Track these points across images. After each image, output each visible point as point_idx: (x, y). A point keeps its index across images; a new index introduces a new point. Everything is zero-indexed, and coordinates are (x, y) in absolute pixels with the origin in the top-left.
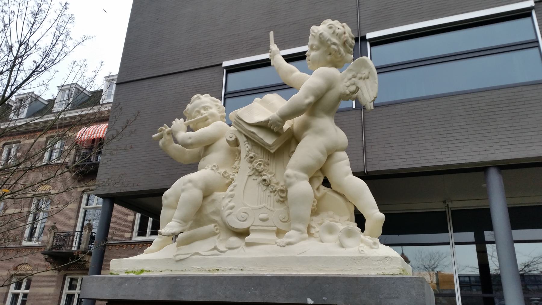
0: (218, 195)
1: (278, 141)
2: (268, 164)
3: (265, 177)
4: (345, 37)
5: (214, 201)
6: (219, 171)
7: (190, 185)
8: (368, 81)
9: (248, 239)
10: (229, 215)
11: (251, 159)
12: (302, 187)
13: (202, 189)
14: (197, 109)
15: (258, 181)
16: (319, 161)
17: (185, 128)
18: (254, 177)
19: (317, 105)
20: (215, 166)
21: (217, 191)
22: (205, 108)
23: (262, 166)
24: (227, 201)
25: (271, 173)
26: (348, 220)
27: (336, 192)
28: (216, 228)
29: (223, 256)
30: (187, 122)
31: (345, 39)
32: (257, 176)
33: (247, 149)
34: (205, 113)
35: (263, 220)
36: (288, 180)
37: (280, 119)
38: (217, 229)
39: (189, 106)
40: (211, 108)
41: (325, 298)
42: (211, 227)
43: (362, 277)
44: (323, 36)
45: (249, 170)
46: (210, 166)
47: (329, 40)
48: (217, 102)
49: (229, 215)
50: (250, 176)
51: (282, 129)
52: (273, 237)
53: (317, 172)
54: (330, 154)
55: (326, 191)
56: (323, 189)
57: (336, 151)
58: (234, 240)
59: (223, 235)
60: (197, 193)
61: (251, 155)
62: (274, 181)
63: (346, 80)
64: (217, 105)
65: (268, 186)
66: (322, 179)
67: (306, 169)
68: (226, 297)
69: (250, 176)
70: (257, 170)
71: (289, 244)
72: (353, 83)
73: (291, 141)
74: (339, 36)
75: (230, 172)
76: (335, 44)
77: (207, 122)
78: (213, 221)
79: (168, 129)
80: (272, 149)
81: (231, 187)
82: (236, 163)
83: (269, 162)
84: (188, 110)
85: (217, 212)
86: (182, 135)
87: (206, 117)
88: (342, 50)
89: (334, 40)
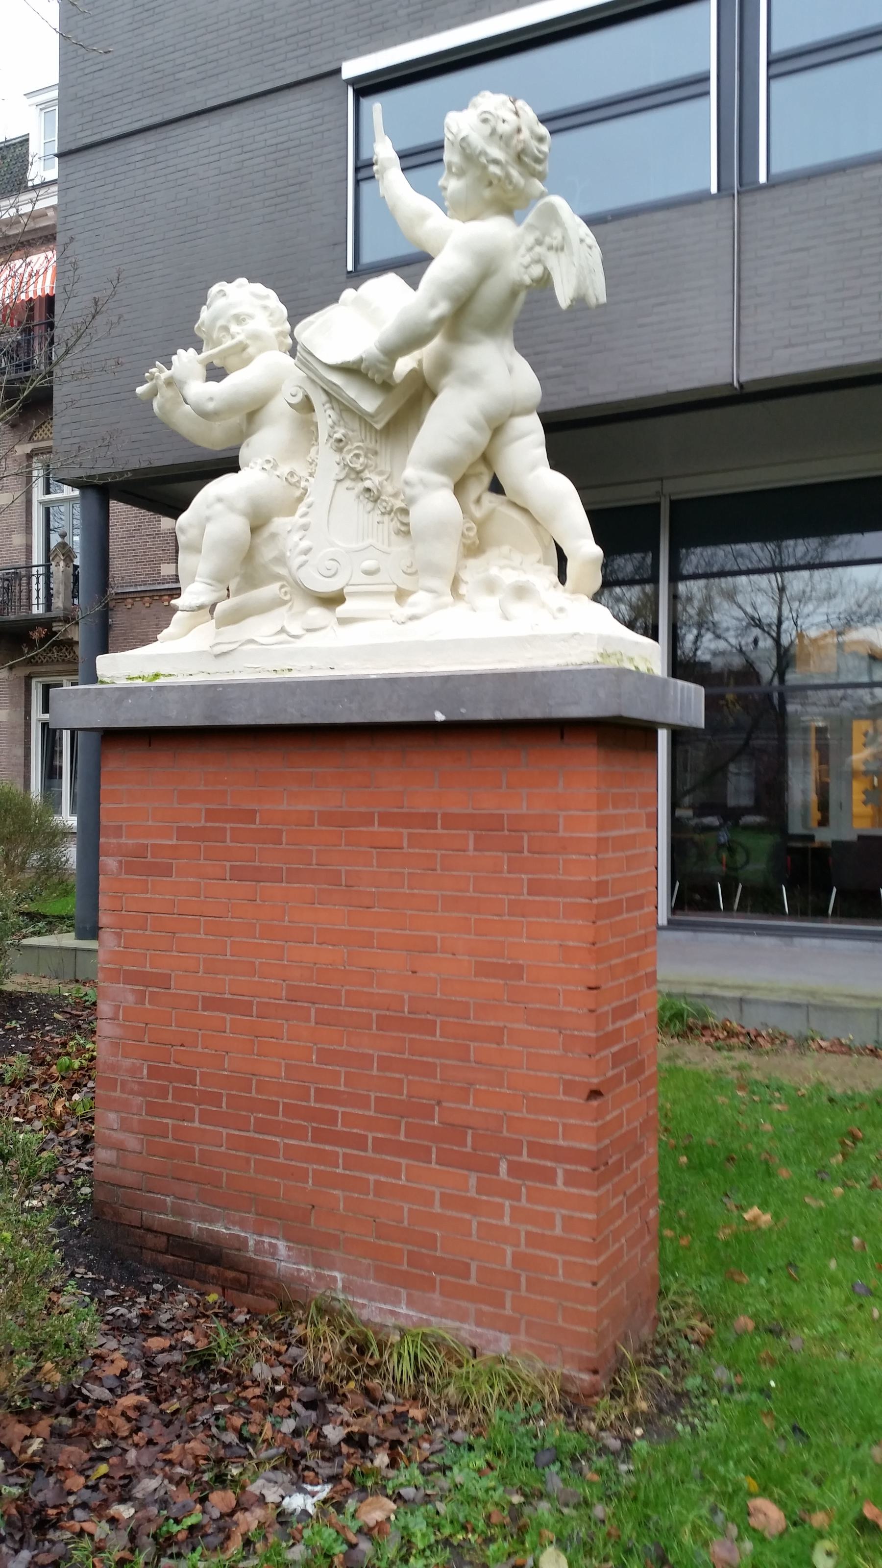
0: (279, 523)
1: (391, 400)
2: (376, 453)
3: (368, 484)
4: (519, 141)
5: (274, 536)
6: (278, 473)
7: (219, 507)
8: (562, 255)
9: (342, 610)
10: (301, 566)
11: (340, 445)
12: (438, 502)
13: (245, 514)
14: (221, 322)
15: (356, 491)
16: (470, 445)
17: (201, 371)
18: (348, 483)
19: (463, 317)
20: (268, 461)
21: (279, 514)
22: (239, 319)
23: (362, 459)
24: (295, 537)
25: (381, 473)
26: (539, 562)
27: (515, 505)
28: (283, 590)
29: (298, 644)
30: (204, 354)
31: (520, 147)
32: (353, 480)
33: (330, 421)
34: (240, 333)
35: (368, 573)
36: (409, 491)
37: (382, 357)
38: (286, 593)
39: (205, 314)
40: (251, 317)
41: (463, 711)
42: (271, 590)
43: (524, 673)
44: (469, 145)
45: (337, 469)
46: (260, 461)
47: (483, 153)
48: (267, 297)
49: (301, 566)
50: (339, 481)
51: (391, 376)
52: (390, 604)
53: (472, 465)
54: (497, 427)
55: (493, 505)
56: (491, 500)
57: (513, 415)
58: (317, 614)
59: (298, 604)
60: (238, 525)
61: (338, 436)
62: (389, 489)
63: (523, 250)
64: (265, 308)
65: (375, 501)
66: (486, 480)
67: (443, 466)
68: (303, 716)
69: (339, 481)
70: (352, 469)
71: (412, 618)
72: (536, 258)
73: (413, 400)
74: (504, 140)
75: (302, 470)
76: (496, 162)
77: (245, 355)
78: (277, 577)
79: (167, 373)
80: (376, 422)
81: (302, 508)
82: (313, 450)
83: (378, 448)
84: (203, 323)
85: (281, 560)
86: (199, 389)
87: (241, 342)
88: (514, 173)
89: (496, 152)
